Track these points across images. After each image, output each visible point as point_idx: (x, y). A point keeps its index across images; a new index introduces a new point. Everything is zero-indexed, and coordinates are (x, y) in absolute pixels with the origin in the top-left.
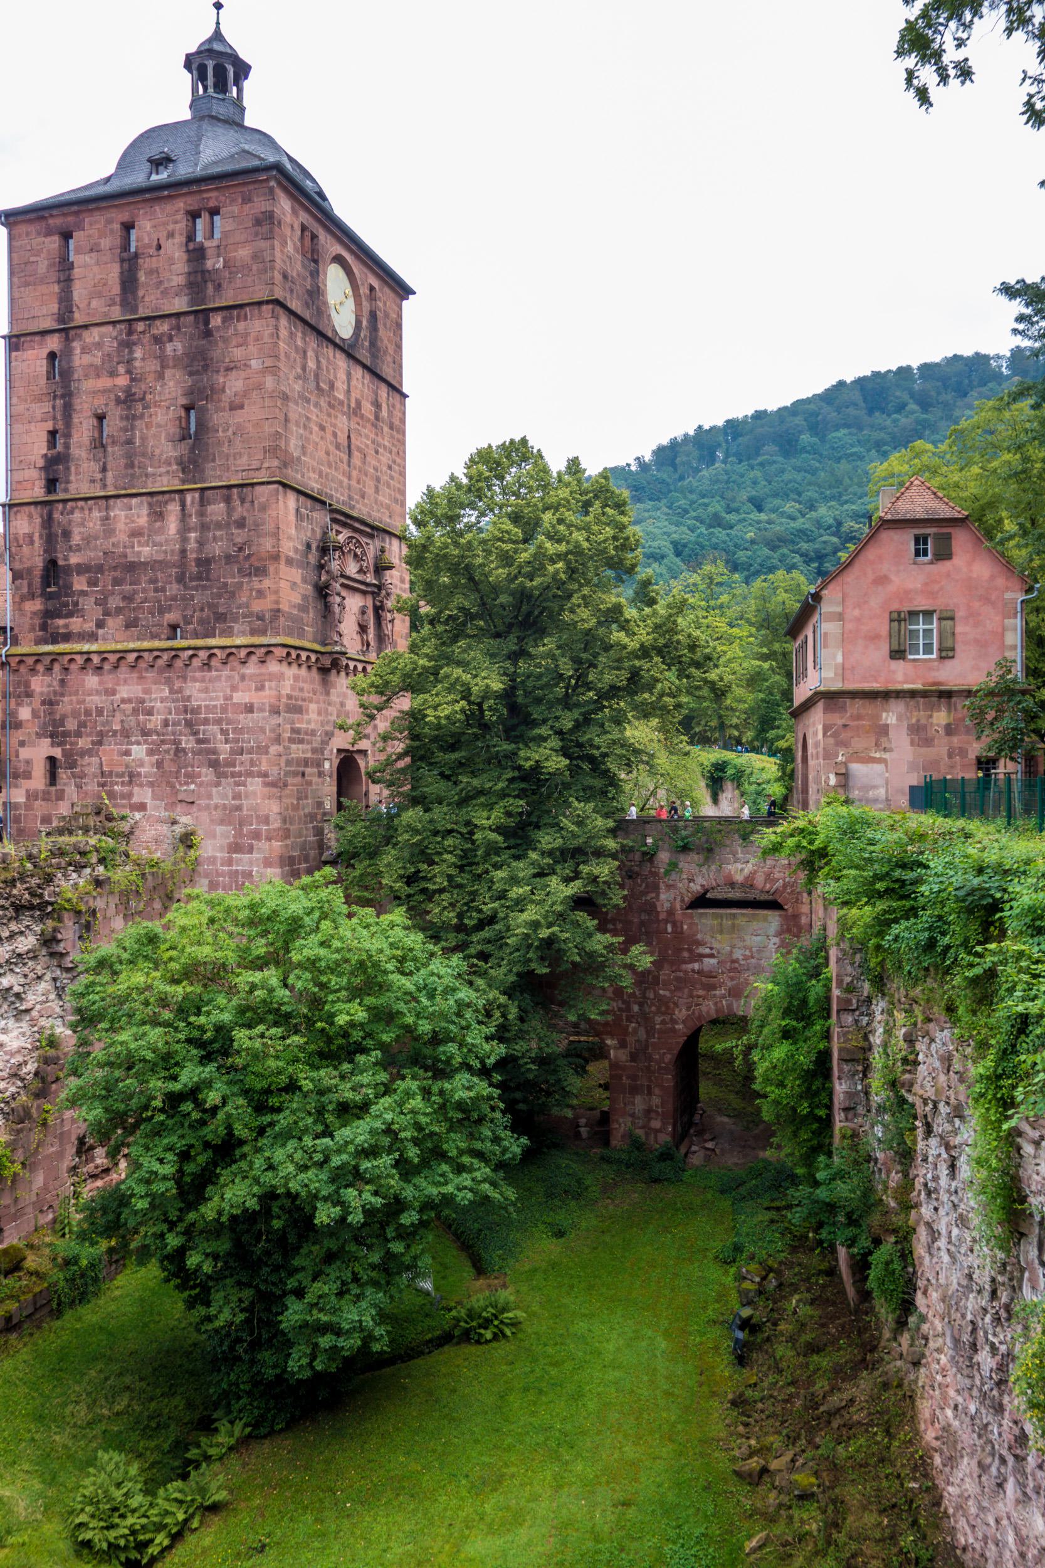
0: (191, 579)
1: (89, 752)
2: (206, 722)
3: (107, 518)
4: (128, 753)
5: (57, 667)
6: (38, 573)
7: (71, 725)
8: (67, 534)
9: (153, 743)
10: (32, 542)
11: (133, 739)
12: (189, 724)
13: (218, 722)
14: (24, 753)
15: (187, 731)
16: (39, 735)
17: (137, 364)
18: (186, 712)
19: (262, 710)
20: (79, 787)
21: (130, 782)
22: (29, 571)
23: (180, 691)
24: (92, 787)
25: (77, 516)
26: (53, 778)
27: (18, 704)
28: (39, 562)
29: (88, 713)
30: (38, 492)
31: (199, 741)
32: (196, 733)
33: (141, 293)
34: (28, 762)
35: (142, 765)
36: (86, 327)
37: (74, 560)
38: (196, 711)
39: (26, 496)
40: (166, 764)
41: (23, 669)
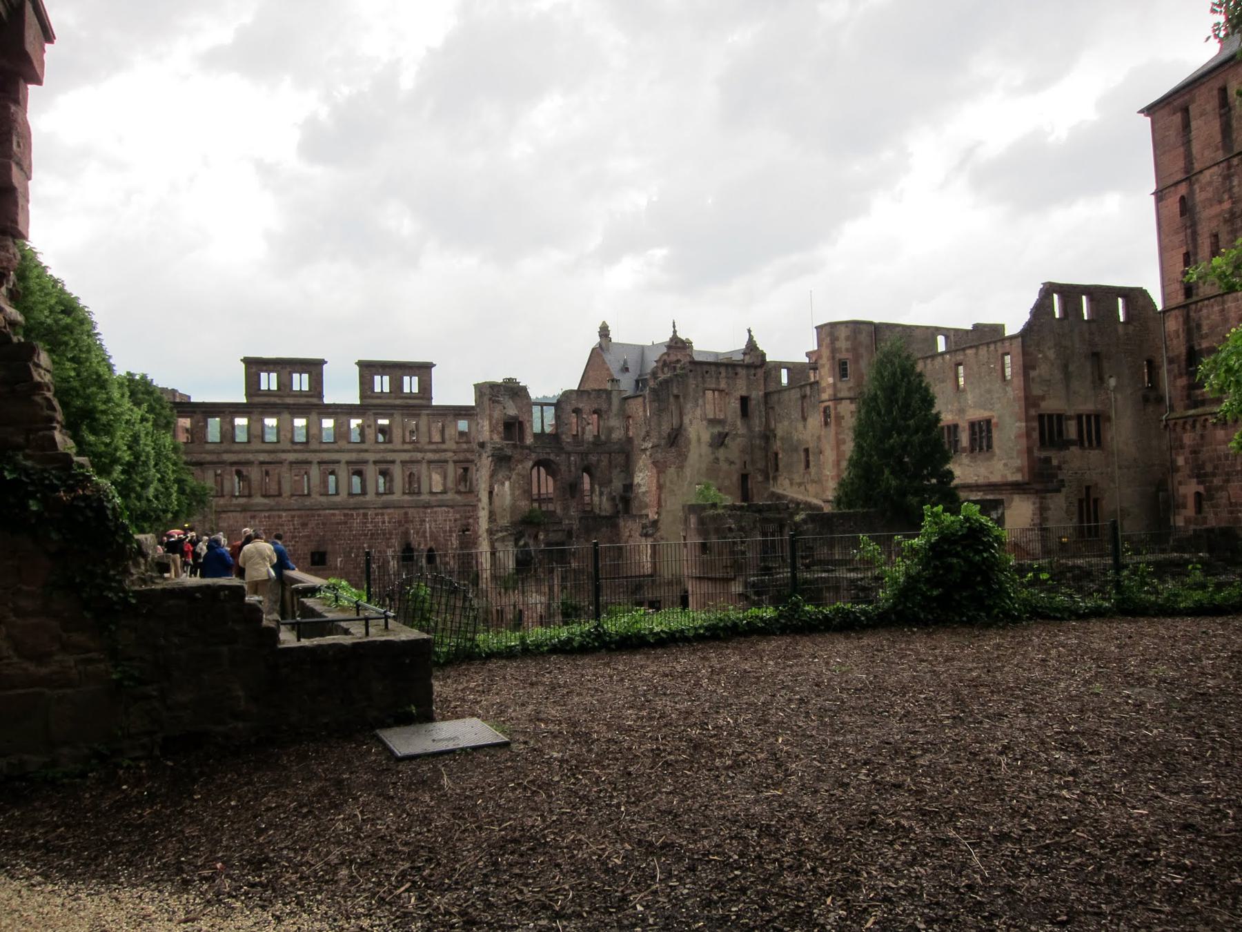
1: (1221, 488)
3: (1223, 310)
5: (1198, 426)
6: (1183, 357)
7: (1209, 468)
8: (1199, 326)
10: (1178, 337)
14: (1182, 490)
16: (1190, 477)
17: (1236, 190)
20: (1216, 514)
22: (1178, 356)
24: (1225, 515)
25: (1205, 311)
26: (1199, 509)
27: (1177, 454)
28: (1183, 350)
29: (1219, 458)
30: (1180, 299)
33: (1234, 136)
34: (1185, 496)
36: (1201, 172)
37: (1205, 345)
39: (1174, 303)
41: (1179, 429)
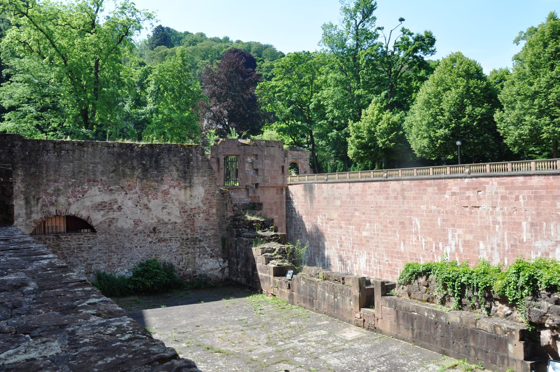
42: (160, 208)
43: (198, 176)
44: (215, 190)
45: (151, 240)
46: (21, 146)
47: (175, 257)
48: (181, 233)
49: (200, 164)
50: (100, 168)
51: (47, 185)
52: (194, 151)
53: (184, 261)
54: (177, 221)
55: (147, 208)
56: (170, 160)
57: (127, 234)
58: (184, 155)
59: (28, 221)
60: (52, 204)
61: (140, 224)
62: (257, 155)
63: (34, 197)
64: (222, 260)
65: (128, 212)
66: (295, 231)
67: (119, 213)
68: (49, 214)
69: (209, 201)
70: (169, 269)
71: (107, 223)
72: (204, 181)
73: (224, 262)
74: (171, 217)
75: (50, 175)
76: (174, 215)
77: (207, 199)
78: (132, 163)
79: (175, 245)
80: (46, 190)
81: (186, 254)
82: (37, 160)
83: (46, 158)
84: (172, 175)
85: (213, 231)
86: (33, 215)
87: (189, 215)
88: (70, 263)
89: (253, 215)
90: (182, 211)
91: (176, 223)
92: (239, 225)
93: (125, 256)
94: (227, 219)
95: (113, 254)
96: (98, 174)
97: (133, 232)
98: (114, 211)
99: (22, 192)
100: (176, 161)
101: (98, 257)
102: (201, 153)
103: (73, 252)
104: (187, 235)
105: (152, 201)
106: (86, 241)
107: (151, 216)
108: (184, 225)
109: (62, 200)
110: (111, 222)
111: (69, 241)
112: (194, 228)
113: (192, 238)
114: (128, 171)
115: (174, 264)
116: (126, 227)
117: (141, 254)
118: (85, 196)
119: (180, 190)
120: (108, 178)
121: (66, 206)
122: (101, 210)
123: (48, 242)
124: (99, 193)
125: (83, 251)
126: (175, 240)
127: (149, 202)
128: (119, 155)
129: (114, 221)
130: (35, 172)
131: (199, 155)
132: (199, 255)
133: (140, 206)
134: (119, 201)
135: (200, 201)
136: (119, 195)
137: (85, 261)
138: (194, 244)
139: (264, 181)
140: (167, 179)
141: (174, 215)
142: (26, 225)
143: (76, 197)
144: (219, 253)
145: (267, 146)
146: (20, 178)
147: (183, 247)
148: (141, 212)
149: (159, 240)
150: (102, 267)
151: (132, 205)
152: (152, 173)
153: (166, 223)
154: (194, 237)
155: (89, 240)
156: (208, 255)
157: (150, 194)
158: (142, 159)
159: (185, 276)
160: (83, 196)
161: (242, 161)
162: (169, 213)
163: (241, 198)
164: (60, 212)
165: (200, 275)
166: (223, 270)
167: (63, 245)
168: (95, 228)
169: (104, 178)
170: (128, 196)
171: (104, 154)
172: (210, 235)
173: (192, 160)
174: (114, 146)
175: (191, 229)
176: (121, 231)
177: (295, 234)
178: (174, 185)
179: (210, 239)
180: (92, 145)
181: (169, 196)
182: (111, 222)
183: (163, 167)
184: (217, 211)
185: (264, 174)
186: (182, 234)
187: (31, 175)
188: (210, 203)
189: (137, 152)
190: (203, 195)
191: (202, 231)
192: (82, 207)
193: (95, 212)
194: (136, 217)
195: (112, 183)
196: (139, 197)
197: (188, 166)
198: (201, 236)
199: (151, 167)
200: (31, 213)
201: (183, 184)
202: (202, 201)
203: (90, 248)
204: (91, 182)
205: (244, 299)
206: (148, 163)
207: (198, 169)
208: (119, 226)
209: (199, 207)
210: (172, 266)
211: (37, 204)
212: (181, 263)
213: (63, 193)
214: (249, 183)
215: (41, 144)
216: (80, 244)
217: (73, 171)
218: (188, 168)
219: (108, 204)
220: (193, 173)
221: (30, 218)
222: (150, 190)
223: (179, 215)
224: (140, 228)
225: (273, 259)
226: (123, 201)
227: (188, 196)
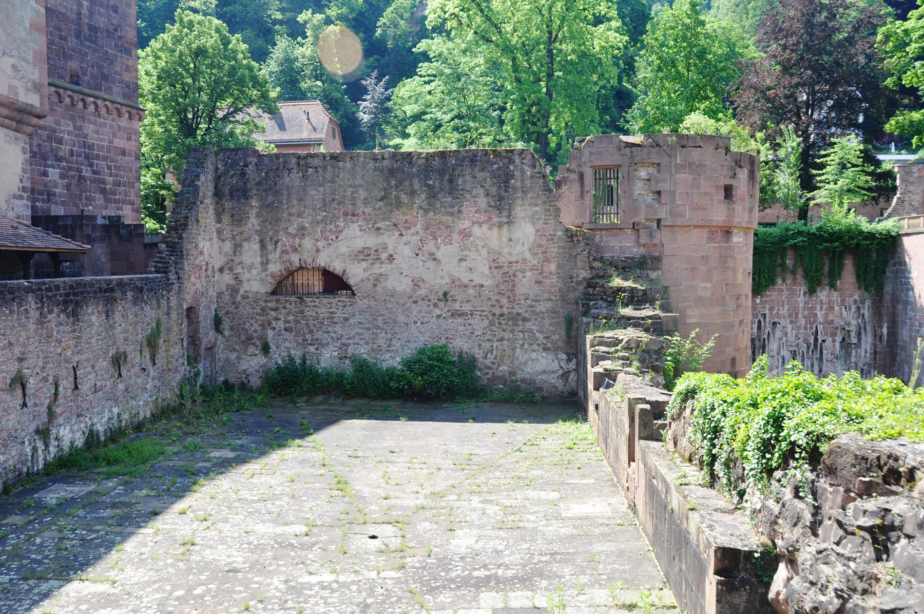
0: (86, 39)
2: (98, 157)
4: (45, 174)
9: (63, 168)
11: (50, 163)
12: (87, 157)
13: (105, 159)
15: (85, 162)
18: (85, 146)
19: (130, 155)
21: (49, 200)
23: (80, 128)
31: (94, 172)
32: (91, 165)
35: (56, 186)
38: (91, 147)
40: (73, 187)
42: (455, 260)
43: (523, 205)
44: (555, 230)
45: (439, 313)
46: (256, 165)
47: (480, 345)
48: (490, 303)
49: (528, 183)
50: (362, 194)
51: (289, 221)
52: (517, 161)
53: (495, 352)
54: (485, 283)
55: (435, 259)
56: (474, 177)
57: (402, 301)
58: (499, 168)
59: (263, 275)
60: (295, 250)
61: (422, 285)
62: (659, 164)
63: (271, 239)
64: (564, 356)
65: (404, 265)
66: (911, 330)
67: (390, 266)
68: (291, 264)
69: (544, 249)
70: (467, 364)
71: (372, 281)
72: (536, 213)
73: (569, 360)
74: (473, 276)
75: (293, 206)
76: (480, 272)
77: (541, 246)
78: (411, 185)
79: (479, 324)
80: (287, 228)
81: (498, 341)
82: (276, 184)
83: (287, 180)
84: (476, 203)
85: (549, 304)
86: (270, 266)
87: (506, 274)
88: (317, 339)
89: (626, 279)
90: (493, 265)
91: (482, 286)
92: (594, 295)
93: (398, 336)
94: (578, 283)
95: (379, 331)
96: (359, 203)
97: (411, 297)
98: (382, 263)
99: (256, 231)
100: (485, 179)
101: (357, 333)
102: (530, 163)
103: (322, 323)
104: (501, 307)
105: (443, 247)
106: (340, 308)
107: (440, 273)
108: (496, 290)
109: (308, 243)
110: (377, 280)
111: (316, 306)
112: (515, 296)
113: (509, 313)
114: (404, 198)
115: (477, 356)
116: (399, 289)
117: (423, 334)
118: (340, 238)
119: (490, 229)
120: (374, 209)
121: (313, 253)
122: (363, 260)
123: (288, 305)
124: (359, 233)
125: (336, 323)
126: (480, 315)
127: (438, 248)
128: (392, 172)
129: (381, 279)
130: (273, 202)
131: (526, 168)
132: (523, 345)
133: (423, 255)
134: (390, 247)
135: (526, 248)
136: (389, 236)
137: (338, 339)
138: (514, 325)
139: (673, 214)
140: (468, 209)
141: (480, 272)
142: (262, 280)
143: (326, 239)
144: (560, 344)
145: (683, 147)
146: (255, 211)
147: (494, 328)
148: (424, 266)
149: (452, 315)
150: (363, 351)
151: (411, 254)
152: (443, 200)
153: (466, 286)
154: (514, 312)
155: (345, 306)
156: (538, 345)
157: (440, 236)
158: (428, 177)
159: (495, 378)
160: (337, 238)
161: (626, 176)
162: (471, 269)
163: (624, 245)
164: (305, 262)
165: (523, 381)
166: (565, 375)
167: (309, 312)
168: (354, 288)
169: (368, 210)
170: (404, 238)
171: (368, 171)
172: (544, 310)
173: (512, 177)
174: (383, 158)
175: (509, 297)
176: (392, 296)
177: (911, 337)
178: (481, 220)
179: (543, 318)
180: (351, 158)
181: (471, 239)
182: (377, 279)
183: (462, 190)
184: (559, 267)
185: (673, 201)
186: (493, 306)
187: (268, 206)
188: (546, 252)
189: (420, 166)
190: (532, 238)
191: (529, 302)
192: (334, 255)
193: (353, 264)
194: (416, 274)
195: (381, 217)
196: (421, 240)
197: (506, 187)
198: (526, 312)
199: (441, 189)
200: (268, 262)
201: (496, 220)
202: (530, 250)
203: (346, 319)
204: (349, 217)
205: (543, 426)
206: (437, 184)
207: (523, 192)
208: (390, 287)
209: (524, 260)
210: (474, 360)
211: (276, 247)
212: (489, 355)
213: (309, 234)
214: (641, 218)
215: (281, 160)
216: (331, 313)
217: (324, 200)
218: (506, 191)
219: (372, 252)
220: (514, 200)
221: (266, 270)
222: (439, 229)
223: (487, 272)
224: (422, 292)
225: (608, 359)
226: (395, 247)
227: (505, 240)
